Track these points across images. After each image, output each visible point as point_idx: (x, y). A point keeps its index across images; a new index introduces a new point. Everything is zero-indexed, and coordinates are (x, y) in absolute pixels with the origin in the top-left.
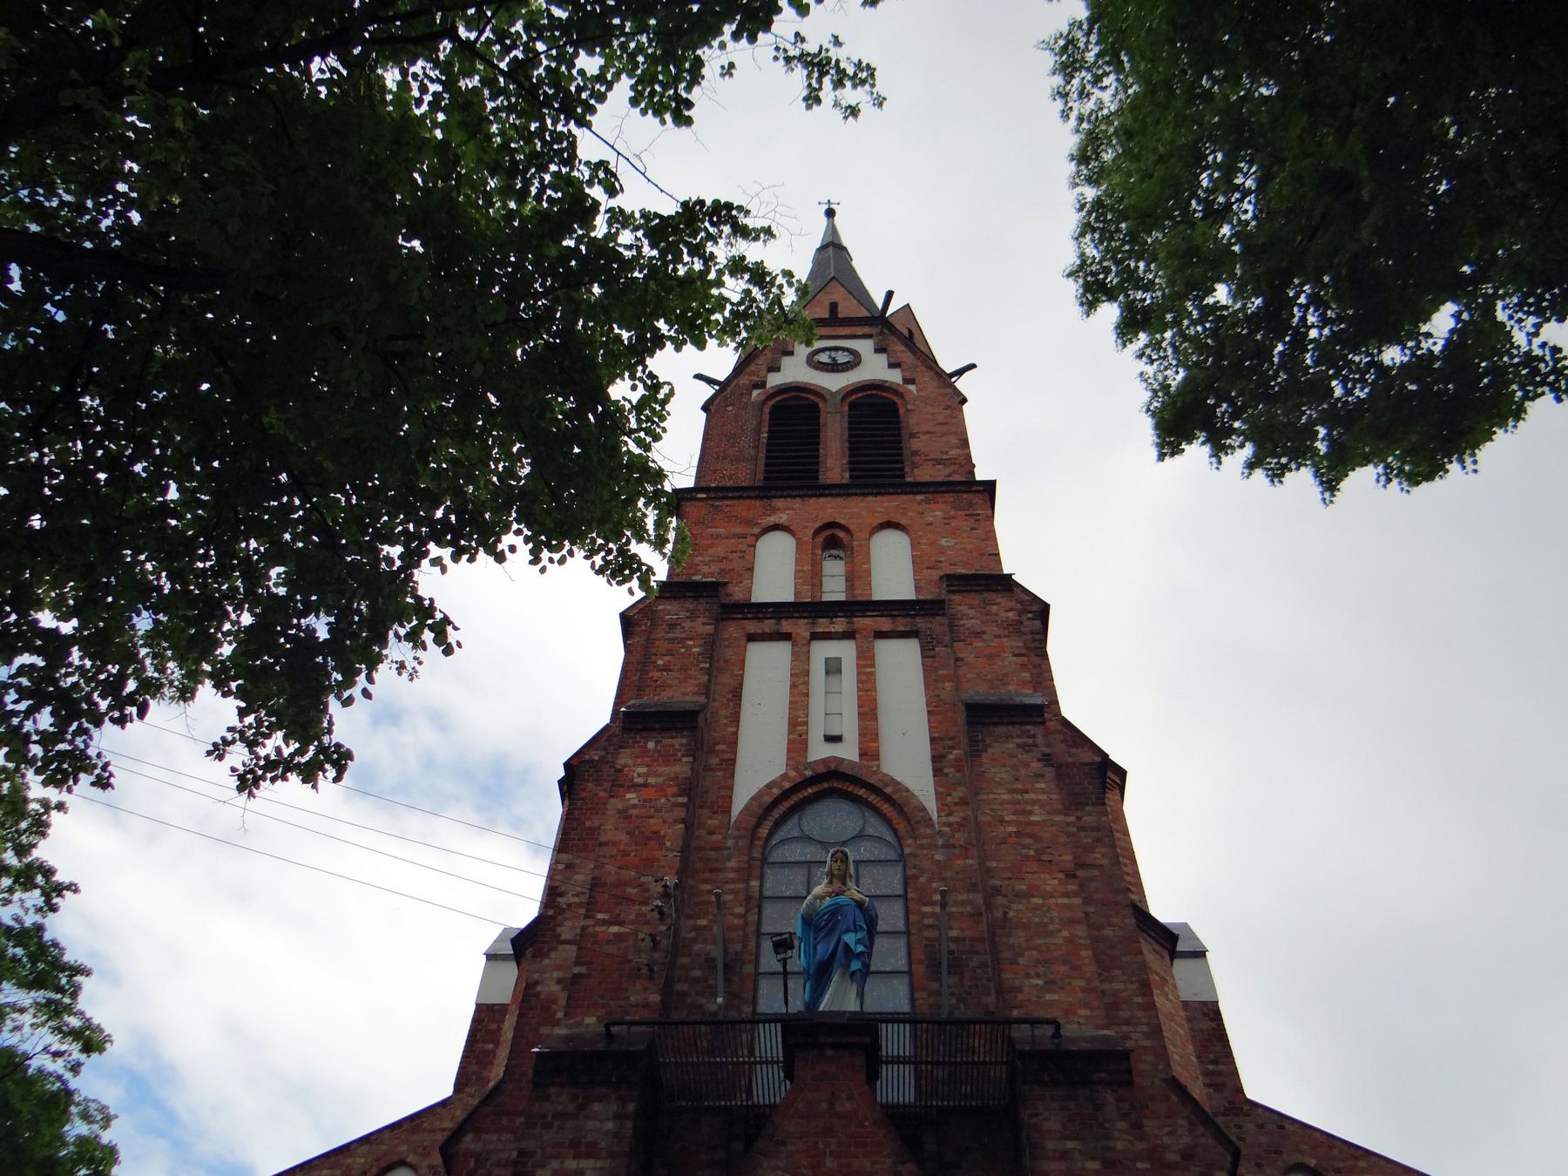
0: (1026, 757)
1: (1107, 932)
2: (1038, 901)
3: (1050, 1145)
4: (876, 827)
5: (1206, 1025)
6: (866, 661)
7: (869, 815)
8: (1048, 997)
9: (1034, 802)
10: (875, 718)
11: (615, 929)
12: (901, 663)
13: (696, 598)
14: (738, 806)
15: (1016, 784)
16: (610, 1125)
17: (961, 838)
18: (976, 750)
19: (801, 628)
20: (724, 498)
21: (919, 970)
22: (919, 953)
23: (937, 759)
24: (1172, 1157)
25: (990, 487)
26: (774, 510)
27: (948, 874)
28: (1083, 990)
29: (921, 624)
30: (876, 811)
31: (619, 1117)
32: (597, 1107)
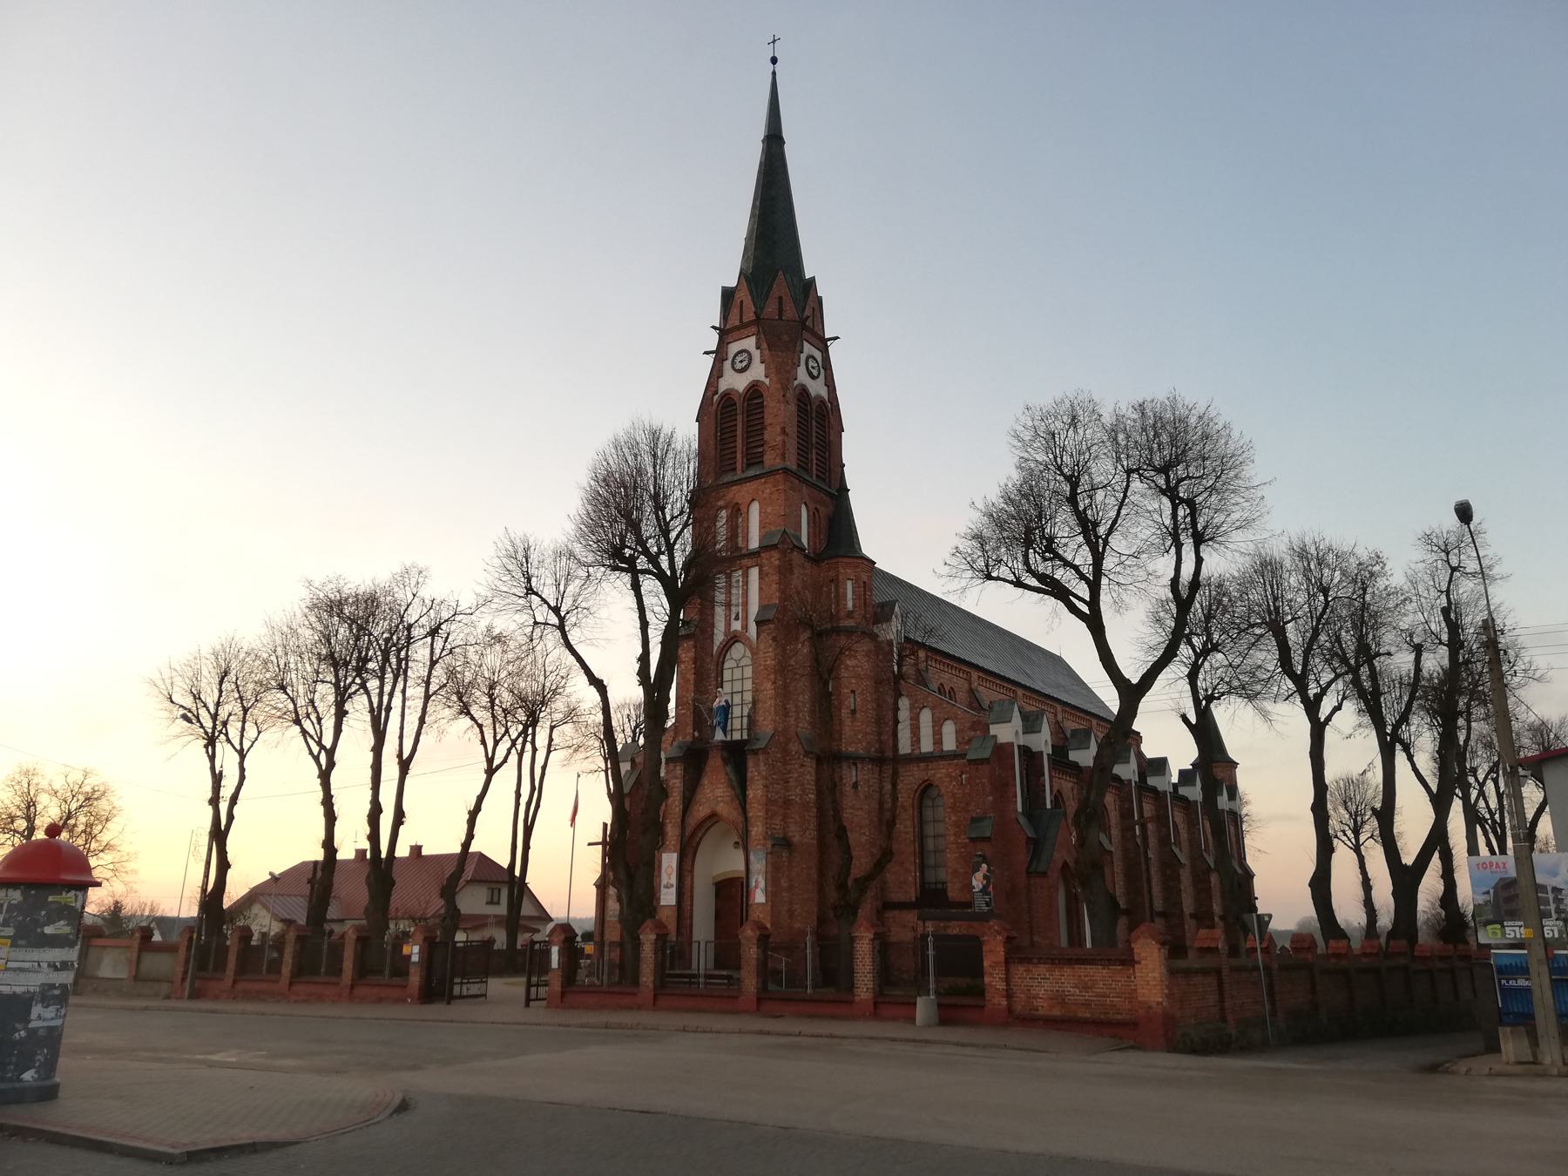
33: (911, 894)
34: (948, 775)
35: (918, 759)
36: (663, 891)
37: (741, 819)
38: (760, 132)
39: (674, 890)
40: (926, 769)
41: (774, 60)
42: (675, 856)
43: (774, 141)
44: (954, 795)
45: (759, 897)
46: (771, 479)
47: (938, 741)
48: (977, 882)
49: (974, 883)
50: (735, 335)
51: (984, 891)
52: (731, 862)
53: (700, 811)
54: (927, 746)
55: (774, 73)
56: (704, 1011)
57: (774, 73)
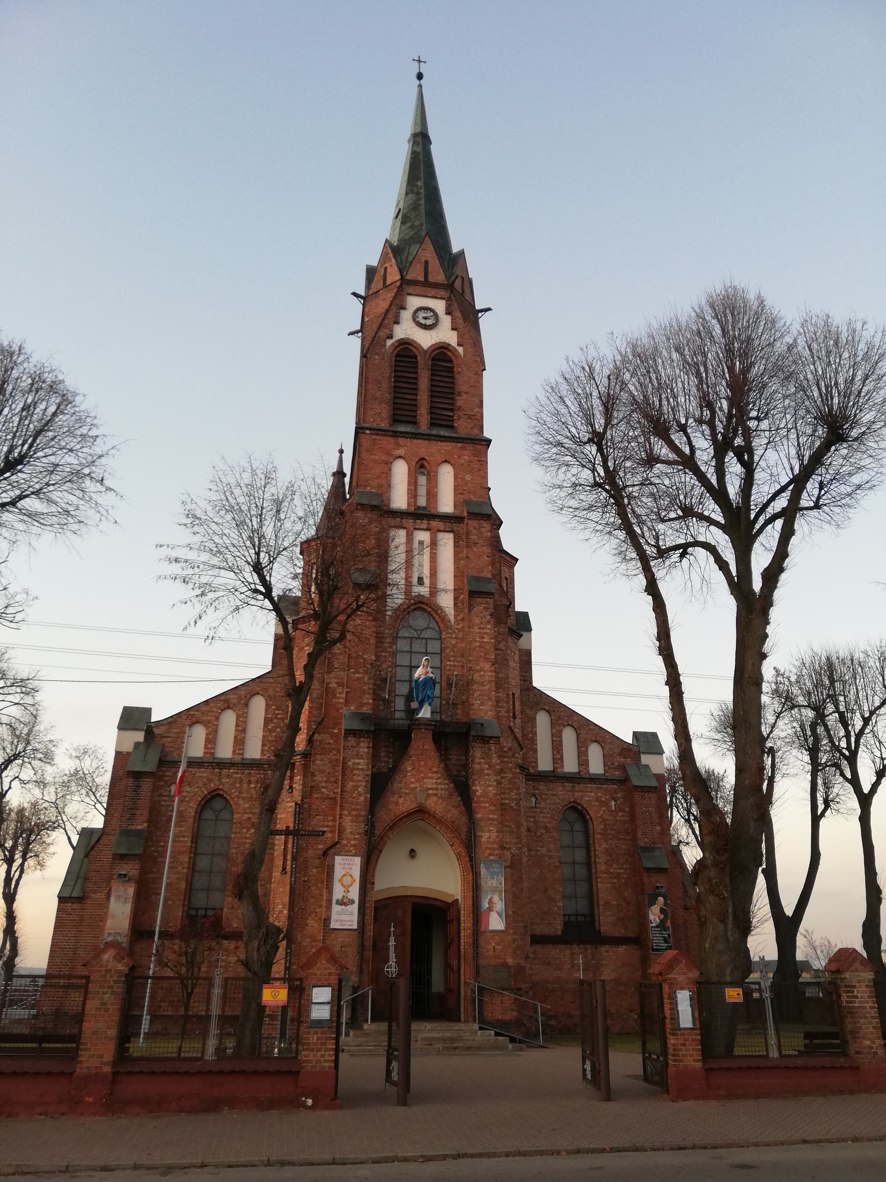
0: (485, 613)
1: (500, 675)
3: (477, 760)
4: (433, 624)
5: (526, 658)
6: (434, 544)
9: (486, 633)
10: (436, 578)
11: (357, 675)
12: (447, 541)
13: (372, 510)
15: (483, 630)
16: (366, 750)
17: (460, 635)
18: (471, 608)
19: (409, 523)
22: (444, 678)
24: (506, 749)
25: (488, 442)
26: (398, 446)
29: (455, 527)
30: (434, 618)
31: (368, 747)
32: (362, 744)
33: (557, 928)
34: (597, 800)
35: (555, 777)
36: (336, 908)
37: (465, 819)
38: (406, 128)
40: (573, 790)
41: (420, 76)
42: (357, 861)
43: (421, 140)
44: (604, 821)
45: (496, 923)
46: (471, 447)
47: (583, 761)
48: (654, 915)
49: (651, 917)
50: (419, 289)
51: (662, 925)
52: (433, 873)
53: (401, 802)
54: (570, 765)
55: (420, 86)
57: (420, 86)
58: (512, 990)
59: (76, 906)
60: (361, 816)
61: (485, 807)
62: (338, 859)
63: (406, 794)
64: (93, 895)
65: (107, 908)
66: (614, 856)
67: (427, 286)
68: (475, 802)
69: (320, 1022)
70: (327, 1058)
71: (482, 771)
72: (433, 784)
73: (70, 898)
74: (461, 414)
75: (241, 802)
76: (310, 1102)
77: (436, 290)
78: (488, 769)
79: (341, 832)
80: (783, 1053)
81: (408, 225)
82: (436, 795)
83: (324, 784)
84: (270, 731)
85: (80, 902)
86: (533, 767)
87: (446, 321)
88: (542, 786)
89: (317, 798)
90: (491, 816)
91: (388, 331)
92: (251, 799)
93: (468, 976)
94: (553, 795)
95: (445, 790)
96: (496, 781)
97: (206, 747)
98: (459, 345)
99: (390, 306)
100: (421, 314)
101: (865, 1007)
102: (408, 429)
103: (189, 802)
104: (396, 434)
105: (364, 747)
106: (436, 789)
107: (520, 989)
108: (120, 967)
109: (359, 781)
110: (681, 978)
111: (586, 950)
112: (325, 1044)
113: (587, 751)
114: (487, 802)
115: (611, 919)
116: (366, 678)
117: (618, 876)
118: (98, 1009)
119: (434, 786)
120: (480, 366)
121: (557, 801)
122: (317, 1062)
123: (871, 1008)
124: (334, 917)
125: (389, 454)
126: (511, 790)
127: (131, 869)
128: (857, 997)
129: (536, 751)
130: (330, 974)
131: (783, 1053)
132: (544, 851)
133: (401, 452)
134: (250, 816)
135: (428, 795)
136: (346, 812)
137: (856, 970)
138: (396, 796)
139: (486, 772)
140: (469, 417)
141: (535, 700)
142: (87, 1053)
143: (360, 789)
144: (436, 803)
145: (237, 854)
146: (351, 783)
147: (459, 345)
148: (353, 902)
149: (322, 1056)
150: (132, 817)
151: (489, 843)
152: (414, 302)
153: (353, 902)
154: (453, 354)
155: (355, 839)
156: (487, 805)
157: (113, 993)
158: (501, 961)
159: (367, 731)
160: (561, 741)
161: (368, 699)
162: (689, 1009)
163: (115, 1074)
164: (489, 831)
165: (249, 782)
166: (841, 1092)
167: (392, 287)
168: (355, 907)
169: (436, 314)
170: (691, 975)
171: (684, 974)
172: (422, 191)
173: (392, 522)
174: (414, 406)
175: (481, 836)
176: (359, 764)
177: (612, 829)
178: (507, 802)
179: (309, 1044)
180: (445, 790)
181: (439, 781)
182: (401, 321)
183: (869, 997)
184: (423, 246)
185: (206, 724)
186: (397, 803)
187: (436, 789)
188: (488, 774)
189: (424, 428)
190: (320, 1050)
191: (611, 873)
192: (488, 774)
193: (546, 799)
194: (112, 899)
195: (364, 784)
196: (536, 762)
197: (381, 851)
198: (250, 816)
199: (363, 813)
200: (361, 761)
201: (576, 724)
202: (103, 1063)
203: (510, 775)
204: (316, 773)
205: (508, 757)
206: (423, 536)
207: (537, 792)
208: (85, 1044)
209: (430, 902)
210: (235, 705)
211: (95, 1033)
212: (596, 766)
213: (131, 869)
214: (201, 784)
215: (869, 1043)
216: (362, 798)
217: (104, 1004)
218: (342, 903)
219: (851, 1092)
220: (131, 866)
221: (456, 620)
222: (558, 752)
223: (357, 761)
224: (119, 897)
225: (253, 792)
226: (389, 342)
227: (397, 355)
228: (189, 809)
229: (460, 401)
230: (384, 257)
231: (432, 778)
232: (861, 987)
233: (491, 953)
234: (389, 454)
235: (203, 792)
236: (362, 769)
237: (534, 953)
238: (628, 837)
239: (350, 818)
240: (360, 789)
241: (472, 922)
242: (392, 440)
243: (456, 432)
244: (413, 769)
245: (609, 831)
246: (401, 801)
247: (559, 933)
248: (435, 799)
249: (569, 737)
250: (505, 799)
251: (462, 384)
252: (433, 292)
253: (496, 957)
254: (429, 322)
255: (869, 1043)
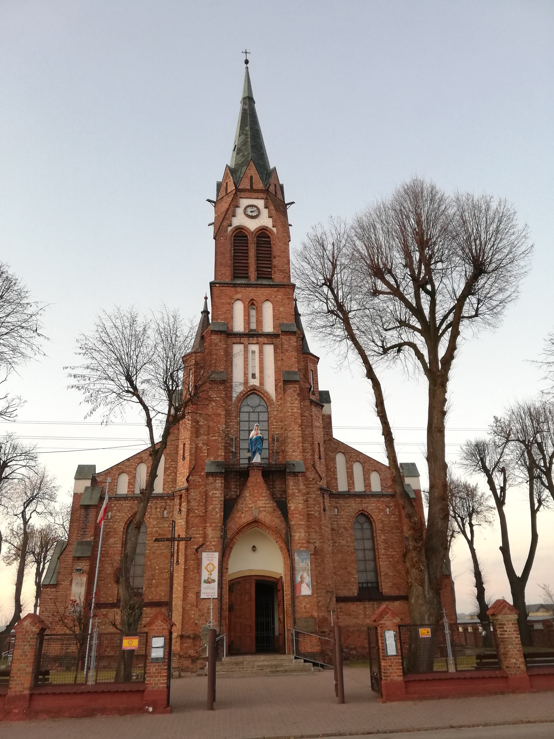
1: (306, 432)
2: (293, 432)
3: (291, 488)
4: (263, 403)
5: (328, 420)
6: (261, 352)
7: (262, 400)
8: (293, 454)
11: (214, 438)
12: (269, 350)
13: (221, 334)
14: (234, 399)
15: (293, 404)
16: (220, 485)
17: (280, 408)
18: (285, 391)
19: (245, 340)
20: (224, 286)
21: (270, 440)
22: (270, 436)
23: (276, 386)
24: (311, 479)
26: (237, 293)
27: (277, 418)
28: (300, 452)
29: (274, 340)
32: (217, 481)
33: (355, 592)
34: (377, 508)
35: (349, 495)
36: (203, 585)
37: (284, 525)
38: (239, 94)
39: (215, 585)
40: (361, 503)
41: (247, 62)
42: (216, 555)
43: (249, 101)
44: (382, 521)
45: (305, 590)
46: (283, 290)
47: (367, 484)
50: (247, 194)
53: (242, 516)
54: (359, 487)
55: (247, 68)
56: (446, 697)
58: (317, 633)
59: (53, 590)
60: (218, 526)
61: (297, 517)
62: (204, 555)
63: (246, 511)
64: (62, 583)
65: (71, 590)
66: (390, 544)
67: (252, 191)
68: (291, 514)
69: (157, 659)
70: (162, 682)
71: (294, 494)
72: (263, 504)
73: (49, 585)
74: (276, 269)
75: (151, 520)
76: (151, 709)
77: (258, 194)
78: (298, 493)
79: (205, 536)
80: (458, 669)
81: (241, 154)
82: (265, 511)
83: (196, 508)
84: (168, 475)
85: (55, 588)
86: (335, 490)
87: (265, 212)
88: (341, 501)
89: (192, 516)
90: (301, 523)
91: (228, 222)
92: (158, 518)
93: (289, 625)
94: (348, 506)
95: (271, 507)
96: (303, 500)
97: (129, 488)
98: (273, 227)
99: (229, 206)
100: (249, 210)
101: (512, 638)
102: (243, 281)
103: (119, 522)
104: (235, 285)
105: (219, 483)
106: (265, 507)
107: (324, 632)
108: (34, 629)
109: (216, 504)
110: (388, 623)
111: (374, 605)
112: (160, 673)
113: (369, 477)
114: (297, 514)
115: (389, 584)
116: (220, 439)
117: (393, 557)
118: (21, 656)
119: (264, 505)
120: (287, 238)
121: (352, 510)
122: (156, 684)
123: (516, 638)
124: (203, 591)
125: (231, 298)
126: (315, 505)
127: (84, 565)
128: (506, 631)
129: (336, 479)
130: (163, 629)
131: (458, 669)
132: (344, 542)
133: (239, 296)
134: (157, 529)
135: (260, 511)
136: (208, 525)
137: (505, 614)
138: (240, 513)
139: (297, 494)
140: (282, 271)
141: (335, 446)
142: (15, 683)
143: (217, 510)
144: (265, 516)
145: (150, 553)
146: (211, 506)
147: (273, 227)
148: (214, 581)
149: (159, 680)
150: (84, 534)
151: (300, 539)
152: (244, 202)
153: (214, 581)
154: (270, 233)
155: (214, 541)
156: (298, 516)
157: (30, 645)
158: (310, 614)
159: (220, 473)
160: (353, 472)
161: (222, 453)
162: (394, 643)
163: (31, 695)
164: (300, 532)
165: (156, 508)
166: (496, 693)
167: (230, 194)
168: (216, 584)
169: (258, 209)
170: (395, 621)
171: (390, 620)
172: (249, 133)
173: (234, 340)
174: (246, 267)
175: (294, 536)
176: (216, 494)
177: (388, 527)
178: (313, 513)
179: (150, 673)
180: (271, 507)
181: (267, 502)
182: (236, 215)
183: (514, 631)
184: (249, 167)
185: (129, 473)
186: (240, 517)
187: (265, 507)
188: (298, 496)
189: (253, 280)
190: (157, 677)
191: (388, 555)
192: (298, 496)
193: (344, 509)
194: (73, 585)
195: (219, 506)
196: (337, 486)
197: (232, 548)
198: (157, 529)
199: (219, 525)
200: (217, 491)
201: (361, 461)
202: (24, 688)
203: (314, 496)
204: (191, 501)
205: (312, 484)
206: (255, 348)
207: (338, 505)
208: (13, 677)
209: (267, 579)
210: (146, 460)
211: (19, 670)
212: (376, 486)
213: (84, 565)
214: (126, 511)
215: (514, 661)
216: (218, 515)
217: (24, 652)
218: (208, 582)
219: (502, 693)
220: (84, 564)
221: (277, 399)
222: (351, 479)
223: (214, 492)
224: (77, 583)
225: (159, 514)
226: (230, 229)
227: (235, 236)
228: (120, 527)
229: (275, 262)
230: (226, 176)
231: (262, 500)
232: (509, 624)
233: (303, 610)
234: (231, 298)
235: (128, 516)
236: (218, 497)
237: (340, 608)
238: (398, 531)
239: (211, 528)
240: (217, 510)
241: (290, 590)
242: (233, 289)
243: (273, 281)
244: (250, 495)
245: (386, 528)
246: (243, 515)
247: (356, 595)
248: (264, 513)
249: (358, 469)
250: (311, 511)
251: (276, 250)
252: (256, 195)
253: (306, 612)
254: (254, 214)
255: (514, 661)
